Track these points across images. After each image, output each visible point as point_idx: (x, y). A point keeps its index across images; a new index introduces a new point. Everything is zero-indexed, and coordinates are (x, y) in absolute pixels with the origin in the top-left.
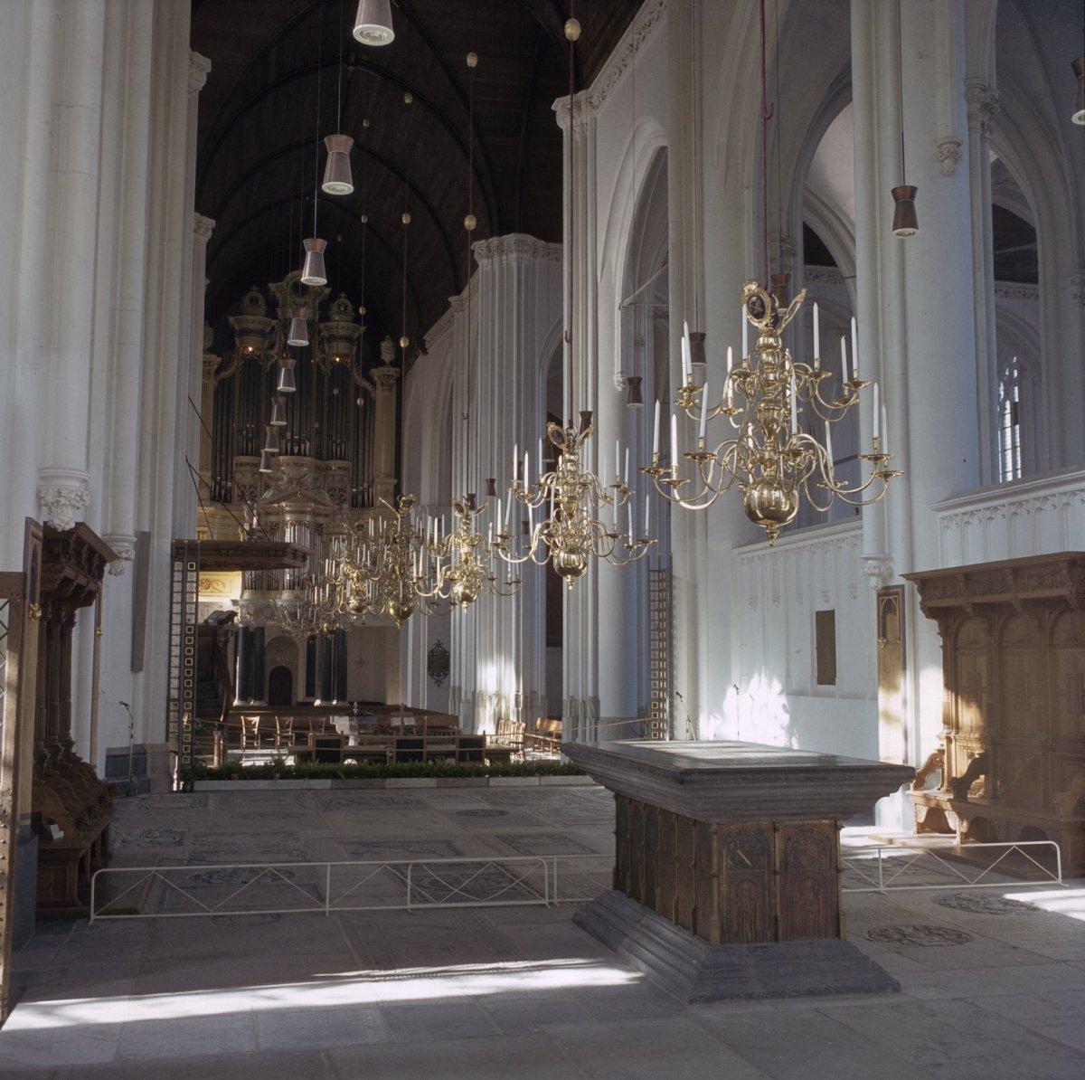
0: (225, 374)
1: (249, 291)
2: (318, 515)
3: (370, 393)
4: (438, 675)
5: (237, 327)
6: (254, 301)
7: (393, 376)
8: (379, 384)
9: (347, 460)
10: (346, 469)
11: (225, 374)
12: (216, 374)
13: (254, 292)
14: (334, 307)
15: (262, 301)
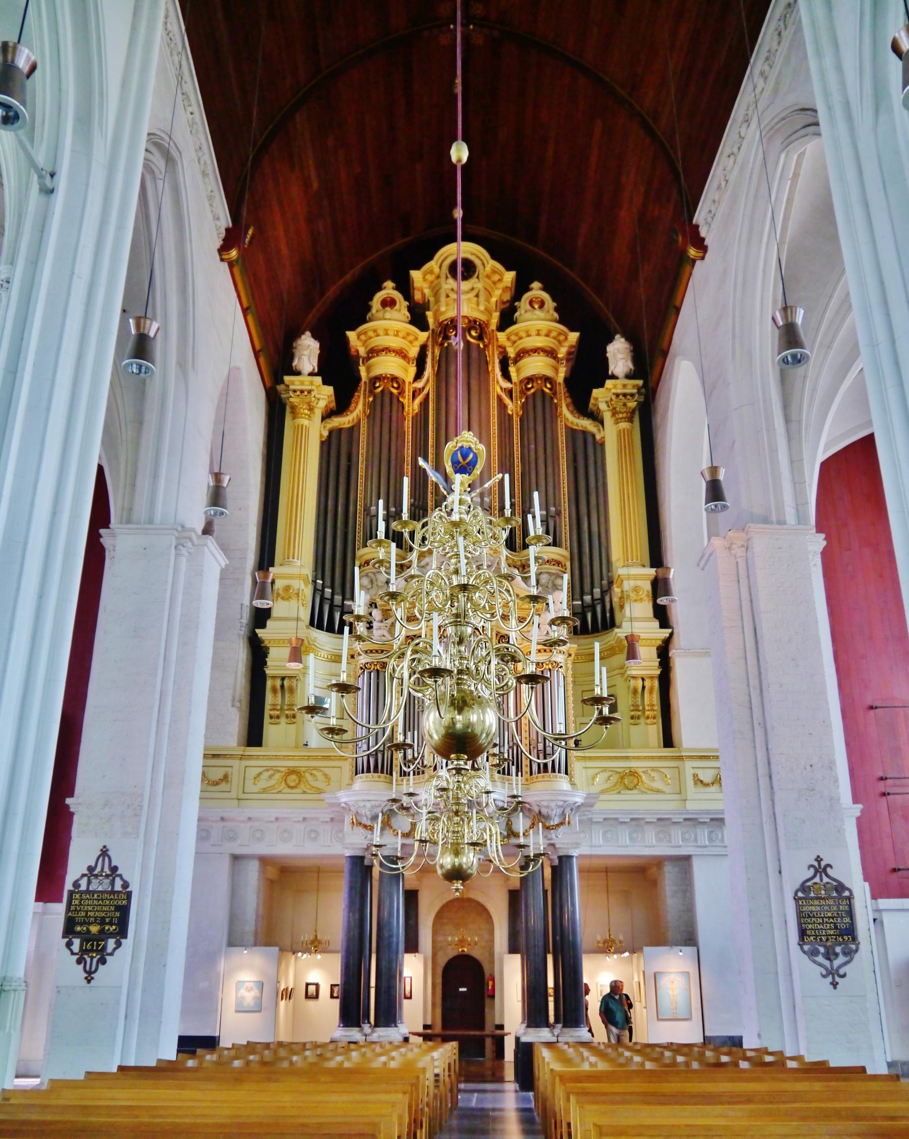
0: (344, 421)
1: (380, 289)
3: (594, 436)
4: (830, 955)
5: (362, 352)
6: (389, 303)
7: (632, 395)
8: (607, 417)
10: (558, 563)
11: (344, 421)
12: (323, 419)
13: (389, 289)
14: (524, 304)
15: (402, 304)
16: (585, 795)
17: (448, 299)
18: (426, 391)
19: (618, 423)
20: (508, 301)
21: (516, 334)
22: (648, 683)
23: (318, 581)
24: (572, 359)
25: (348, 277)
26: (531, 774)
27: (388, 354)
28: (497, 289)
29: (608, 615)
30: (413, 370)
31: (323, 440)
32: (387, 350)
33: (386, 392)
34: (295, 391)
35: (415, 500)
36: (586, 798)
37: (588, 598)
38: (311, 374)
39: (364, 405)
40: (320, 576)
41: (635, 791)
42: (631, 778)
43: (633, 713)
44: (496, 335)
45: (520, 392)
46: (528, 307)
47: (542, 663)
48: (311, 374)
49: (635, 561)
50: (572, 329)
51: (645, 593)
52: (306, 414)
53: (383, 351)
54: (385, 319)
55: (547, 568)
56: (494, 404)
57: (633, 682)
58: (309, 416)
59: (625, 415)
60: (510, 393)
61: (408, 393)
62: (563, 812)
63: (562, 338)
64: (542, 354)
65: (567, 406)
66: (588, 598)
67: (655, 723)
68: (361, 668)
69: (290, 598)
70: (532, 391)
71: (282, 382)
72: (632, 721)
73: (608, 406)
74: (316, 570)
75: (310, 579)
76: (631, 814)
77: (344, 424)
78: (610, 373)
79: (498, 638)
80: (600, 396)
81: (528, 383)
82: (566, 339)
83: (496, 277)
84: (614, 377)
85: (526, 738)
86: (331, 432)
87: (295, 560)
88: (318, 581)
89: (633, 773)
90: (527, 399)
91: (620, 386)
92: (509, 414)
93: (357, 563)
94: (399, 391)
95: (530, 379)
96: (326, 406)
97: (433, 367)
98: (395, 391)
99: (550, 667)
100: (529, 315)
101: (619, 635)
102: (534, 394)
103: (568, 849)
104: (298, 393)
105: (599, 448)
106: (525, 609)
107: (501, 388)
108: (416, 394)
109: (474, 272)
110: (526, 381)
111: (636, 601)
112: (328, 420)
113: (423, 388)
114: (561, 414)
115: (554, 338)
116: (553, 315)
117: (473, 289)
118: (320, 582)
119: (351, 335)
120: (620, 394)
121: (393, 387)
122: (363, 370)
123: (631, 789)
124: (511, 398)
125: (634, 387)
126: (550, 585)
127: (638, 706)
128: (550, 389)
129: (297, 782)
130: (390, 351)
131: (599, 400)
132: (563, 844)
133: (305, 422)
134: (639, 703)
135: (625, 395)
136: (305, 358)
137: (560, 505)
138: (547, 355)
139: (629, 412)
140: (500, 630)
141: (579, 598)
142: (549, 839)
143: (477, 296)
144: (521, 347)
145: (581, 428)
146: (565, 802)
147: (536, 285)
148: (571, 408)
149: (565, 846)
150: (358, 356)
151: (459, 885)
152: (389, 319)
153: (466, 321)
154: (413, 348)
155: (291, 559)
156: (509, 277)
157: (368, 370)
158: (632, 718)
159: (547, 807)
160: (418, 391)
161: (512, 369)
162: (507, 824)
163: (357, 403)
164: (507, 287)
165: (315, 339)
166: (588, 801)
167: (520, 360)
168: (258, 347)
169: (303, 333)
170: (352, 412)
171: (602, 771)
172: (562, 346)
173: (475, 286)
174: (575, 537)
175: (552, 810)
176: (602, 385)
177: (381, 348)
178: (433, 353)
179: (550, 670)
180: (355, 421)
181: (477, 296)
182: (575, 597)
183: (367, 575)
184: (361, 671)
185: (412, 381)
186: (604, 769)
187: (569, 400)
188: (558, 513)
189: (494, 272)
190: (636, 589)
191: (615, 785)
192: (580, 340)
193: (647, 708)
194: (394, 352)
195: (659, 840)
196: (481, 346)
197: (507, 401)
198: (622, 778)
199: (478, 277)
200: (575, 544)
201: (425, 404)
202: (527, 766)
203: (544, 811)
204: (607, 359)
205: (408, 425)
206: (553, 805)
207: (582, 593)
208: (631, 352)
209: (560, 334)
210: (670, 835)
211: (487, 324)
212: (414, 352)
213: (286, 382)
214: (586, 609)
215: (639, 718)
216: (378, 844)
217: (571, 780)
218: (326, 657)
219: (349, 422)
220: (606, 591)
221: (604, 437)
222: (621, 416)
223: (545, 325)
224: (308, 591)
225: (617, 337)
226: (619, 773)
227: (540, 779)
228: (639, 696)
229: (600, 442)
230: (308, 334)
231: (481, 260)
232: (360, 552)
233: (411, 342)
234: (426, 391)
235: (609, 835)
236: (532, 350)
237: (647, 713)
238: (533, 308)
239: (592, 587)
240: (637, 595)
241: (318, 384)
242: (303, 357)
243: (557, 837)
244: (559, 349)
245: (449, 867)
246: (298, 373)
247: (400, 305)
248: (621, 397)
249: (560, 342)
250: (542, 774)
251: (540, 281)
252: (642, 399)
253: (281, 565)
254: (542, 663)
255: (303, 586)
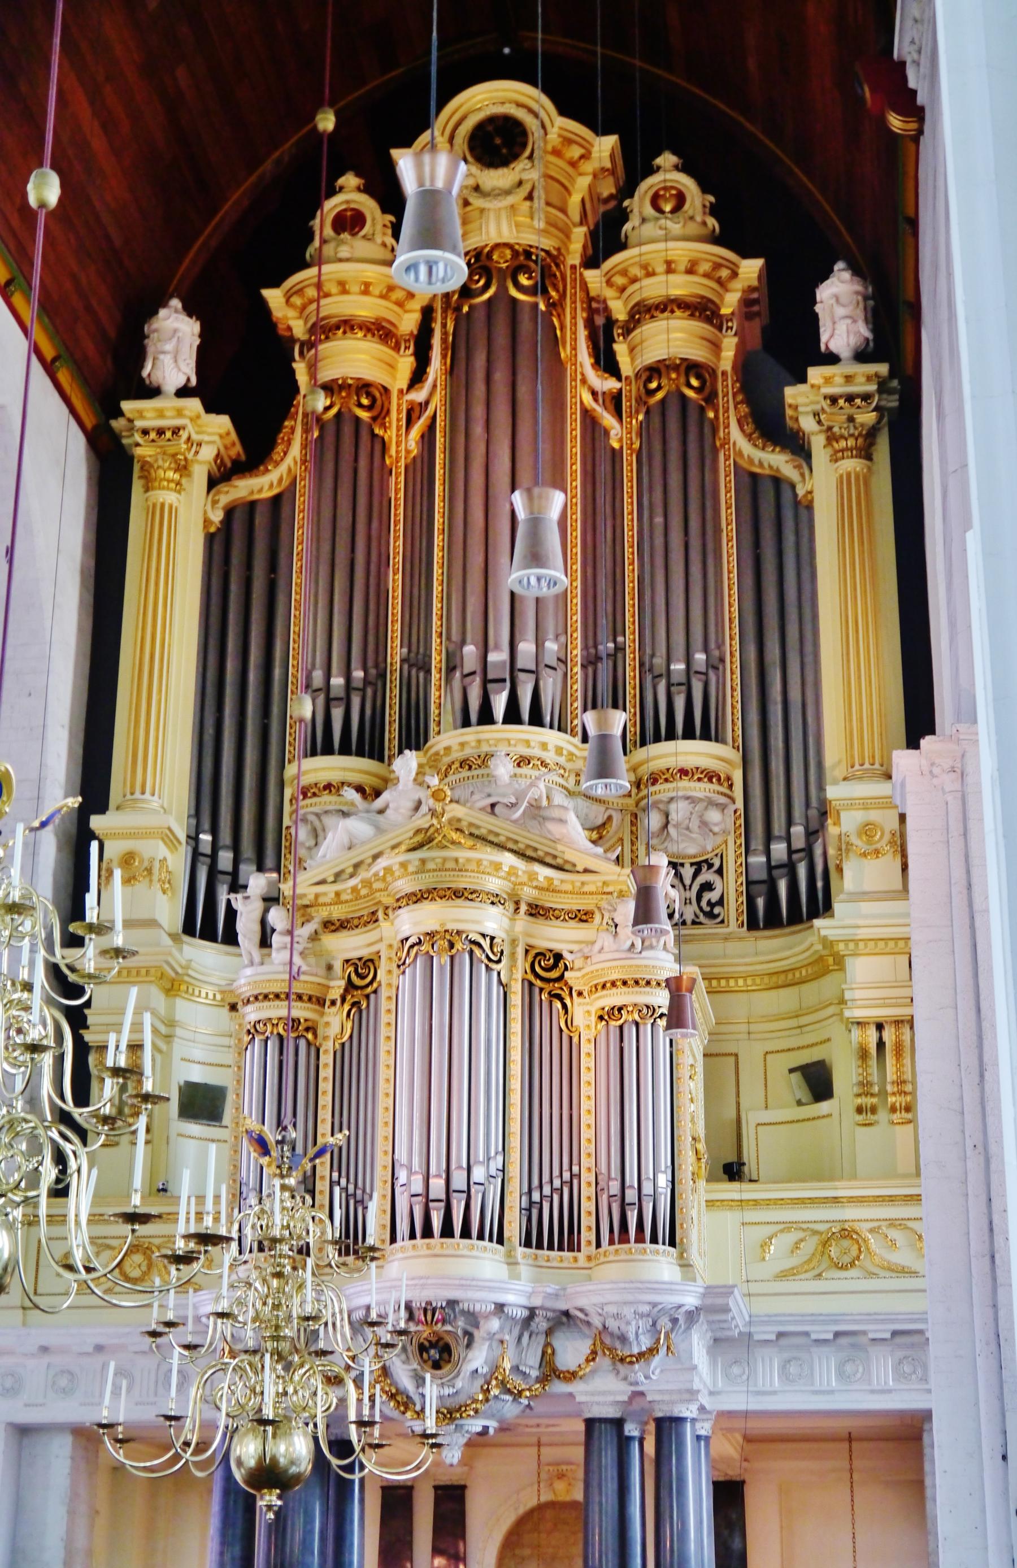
1: (332, 192)
2: (536, 911)
3: (793, 487)
5: (299, 329)
7: (866, 397)
8: (818, 443)
9: (724, 742)
10: (711, 776)
12: (213, 483)
14: (639, 204)
16: (701, 1290)
17: (469, 208)
18: (429, 412)
19: (836, 461)
20: (611, 197)
21: (624, 273)
22: (888, 1035)
23: (201, 836)
24: (758, 314)
25: (268, 166)
26: (598, 1245)
27: (349, 335)
28: (581, 174)
29: (820, 884)
30: (406, 363)
31: (212, 530)
32: (347, 325)
33: (347, 416)
34: (145, 432)
35: (410, 651)
36: (704, 1296)
37: (779, 850)
38: (183, 392)
39: (304, 446)
40: (206, 825)
41: (852, 1273)
42: (846, 1243)
43: (859, 1101)
44: (581, 274)
45: (636, 400)
46: (649, 211)
47: (620, 1009)
48: (183, 392)
49: (867, 766)
50: (746, 254)
51: (887, 837)
52: (169, 481)
53: (338, 328)
54: (341, 260)
55: (685, 789)
56: (574, 430)
57: (856, 1033)
58: (178, 483)
59: (851, 442)
60: (615, 402)
61: (396, 416)
62: (654, 1324)
63: (724, 273)
64: (678, 313)
65: (739, 421)
66: (779, 850)
67: (910, 1122)
68: (249, 1032)
69: (134, 878)
70: (660, 395)
71: (119, 413)
72: (860, 1118)
73: (819, 422)
74: (197, 814)
75: (182, 836)
76: (836, 1322)
77: (260, 491)
78: (823, 348)
79: (530, 958)
80: (800, 400)
81: (649, 380)
82: (735, 274)
83: (575, 152)
84: (832, 359)
85: (589, 1169)
86: (229, 512)
87: (147, 796)
88: (201, 836)
89: (846, 1233)
90: (647, 413)
91: (839, 380)
92: (613, 449)
93: (288, 793)
94: (375, 413)
95: (654, 371)
96: (218, 455)
97: (444, 357)
98: (364, 415)
99: (636, 1017)
100: (649, 230)
101: (823, 933)
102: (663, 401)
103: (673, 1403)
104: (153, 435)
105: (803, 513)
106: (591, 893)
107: (594, 394)
108: (414, 416)
109: (524, 145)
110: (647, 373)
111: (864, 855)
112: (223, 487)
113: (427, 403)
114: (726, 441)
115: (706, 275)
116: (704, 223)
117: (520, 183)
118: (206, 838)
119: (273, 297)
120: (841, 396)
121: (360, 405)
122: (300, 369)
123: (846, 1269)
124: (618, 413)
125: (869, 379)
126: (695, 824)
127: (870, 1084)
128: (698, 390)
129: (144, 1268)
130: (352, 328)
131: (800, 409)
132: (660, 1392)
133: (169, 497)
134: (875, 1078)
135: (850, 398)
136: (167, 360)
137: (720, 646)
138: (692, 315)
139: (860, 435)
140: (533, 942)
141: (761, 848)
142: (631, 1384)
143: (530, 197)
144: (636, 299)
145: (767, 472)
146: (654, 1305)
147: (667, 159)
148: (749, 428)
149: (666, 1398)
150: (292, 340)
151: (274, 1498)
152: (347, 260)
153: (508, 253)
154: (406, 316)
155: (138, 795)
156: (606, 146)
157: (313, 369)
158: (859, 1110)
159: (617, 1316)
160: (417, 410)
161: (620, 349)
162: (544, 1353)
163: (289, 443)
164: (603, 170)
165: (190, 315)
166: (709, 1301)
167: (634, 328)
168: (49, 353)
169: (164, 304)
170: (277, 464)
171: (782, 1231)
172: (727, 290)
173: (525, 176)
174: (754, 717)
175: (628, 1323)
176: (803, 379)
177: (334, 320)
178: (444, 325)
179: (637, 1024)
180: (285, 483)
181: (530, 197)
182: (753, 847)
183: (304, 820)
184: (247, 1038)
185: (405, 387)
186: (788, 1226)
187: (744, 409)
188: (716, 664)
189: (568, 141)
190: (867, 830)
191: (810, 1260)
192: (769, 274)
193: (889, 1088)
194: (361, 329)
195: (900, 1376)
196: (542, 307)
197: (608, 420)
198: (825, 1244)
199: (530, 157)
200: (754, 732)
201: (428, 437)
202: (590, 1228)
203: (613, 1325)
204: (815, 317)
205: (397, 486)
206: (628, 1312)
207: (769, 838)
208: (866, 298)
209: (717, 266)
210: (925, 1367)
211: (555, 258)
212: (409, 323)
213: (128, 415)
214: (776, 873)
215: (874, 1110)
216: (104, 1421)
217: (681, 1256)
218: (211, 996)
219: (271, 486)
220: (817, 832)
221: (811, 492)
222: (843, 444)
223: (682, 251)
224: (178, 861)
225: (839, 265)
226: (815, 1232)
227: (611, 1258)
228: (873, 1062)
229: (805, 503)
230: (176, 303)
231: (536, 115)
232: (290, 770)
233: (400, 304)
234: (429, 412)
235: (793, 1369)
236: (657, 307)
237: (891, 1099)
238: (661, 211)
239: (790, 822)
240: (869, 842)
241: (193, 414)
242: (162, 357)
243: (647, 1377)
244: (721, 297)
245: (252, 1463)
246: (153, 392)
247: (373, 224)
248: (841, 402)
249: (719, 281)
250: (617, 1246)
251: (674, 153)
252: (892, 402)
253: (118, 808)
254: (620, 1009)
255: (162, 850)
